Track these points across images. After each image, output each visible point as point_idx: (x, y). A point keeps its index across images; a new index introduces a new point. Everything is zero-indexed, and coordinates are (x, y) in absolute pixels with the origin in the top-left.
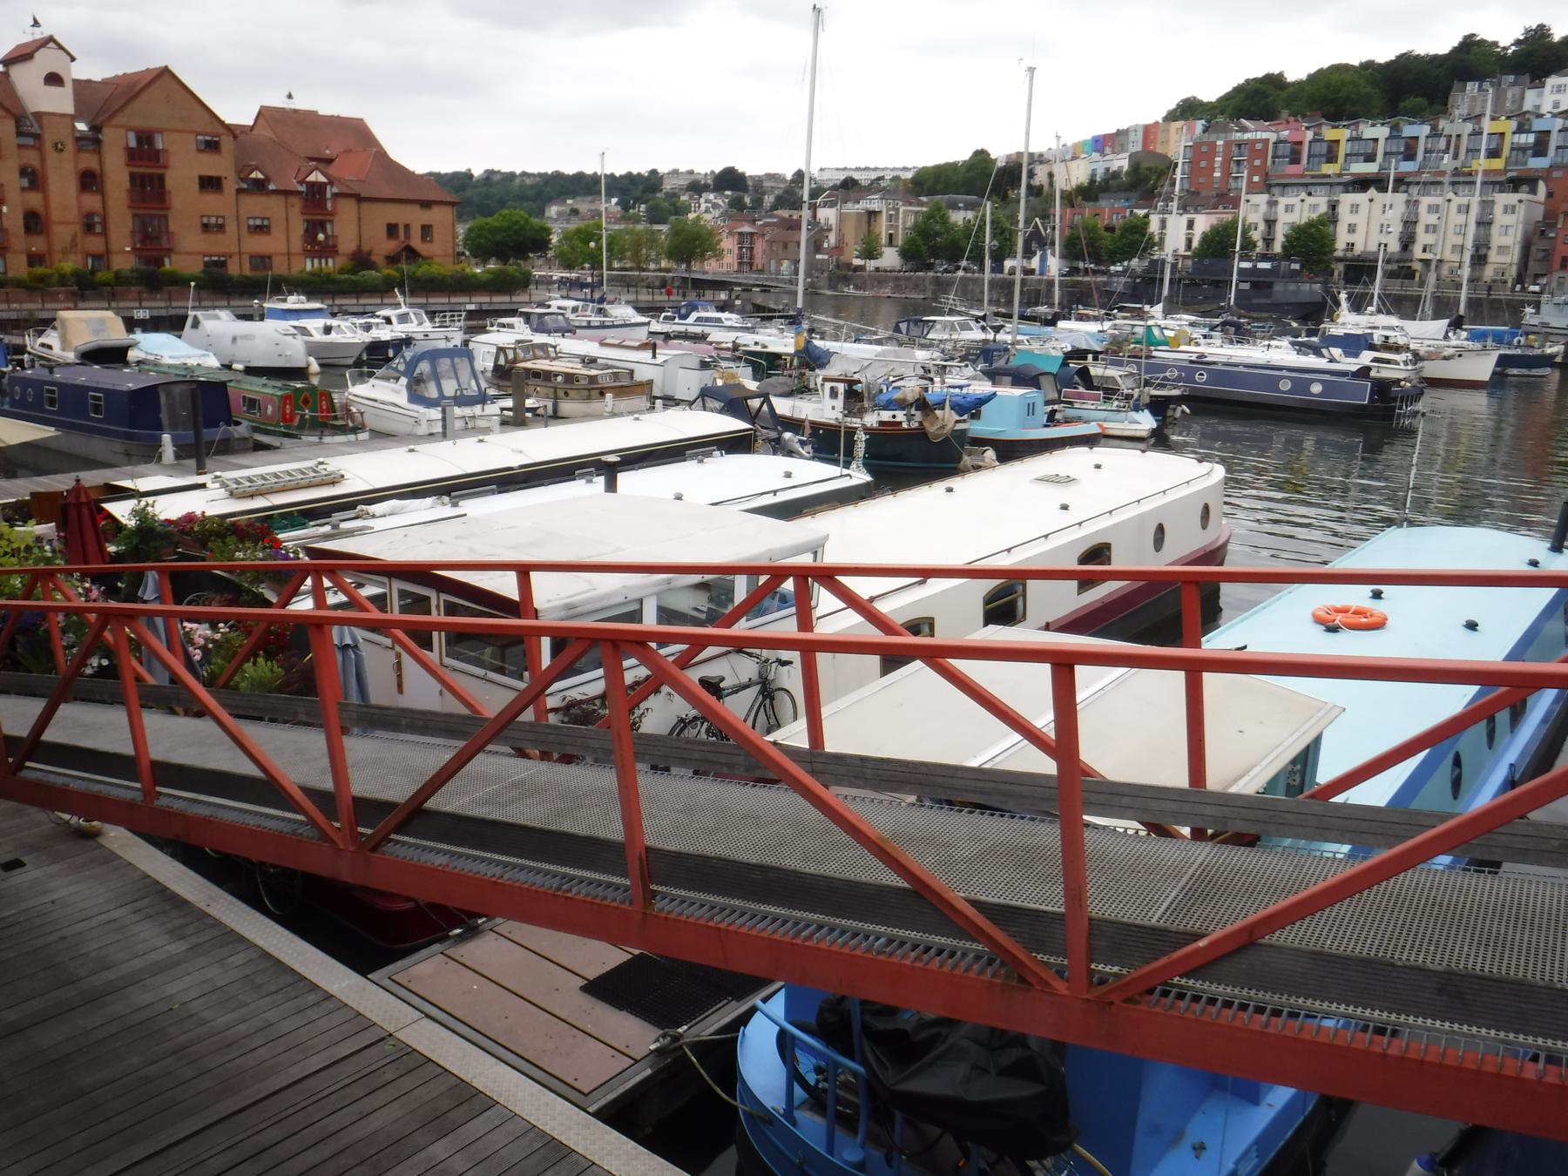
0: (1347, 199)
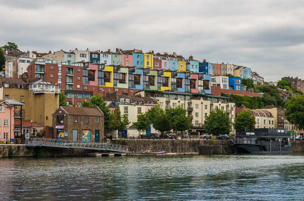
0: (194, 102)
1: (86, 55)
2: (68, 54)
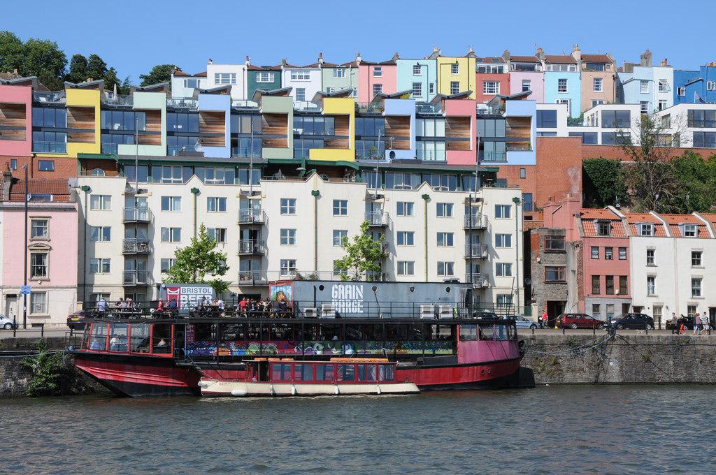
0: (272, 191)
1: (234, 75)
2: (187, 79)
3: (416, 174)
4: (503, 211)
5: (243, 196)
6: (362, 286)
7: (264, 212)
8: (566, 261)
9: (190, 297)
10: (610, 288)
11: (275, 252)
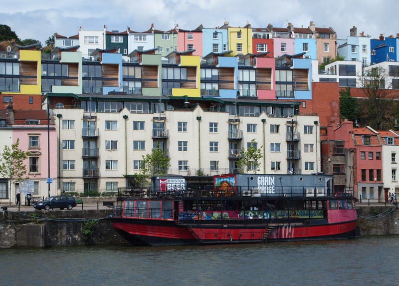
0: (174, 117)
3: (257, 106)
4: (308, 129)
5: (85, 118)
6: (274, 177)
7: (98, 129)
8: (346, 160)
9: (173, 184)
10: (371, 179)
11: (175, 155)
